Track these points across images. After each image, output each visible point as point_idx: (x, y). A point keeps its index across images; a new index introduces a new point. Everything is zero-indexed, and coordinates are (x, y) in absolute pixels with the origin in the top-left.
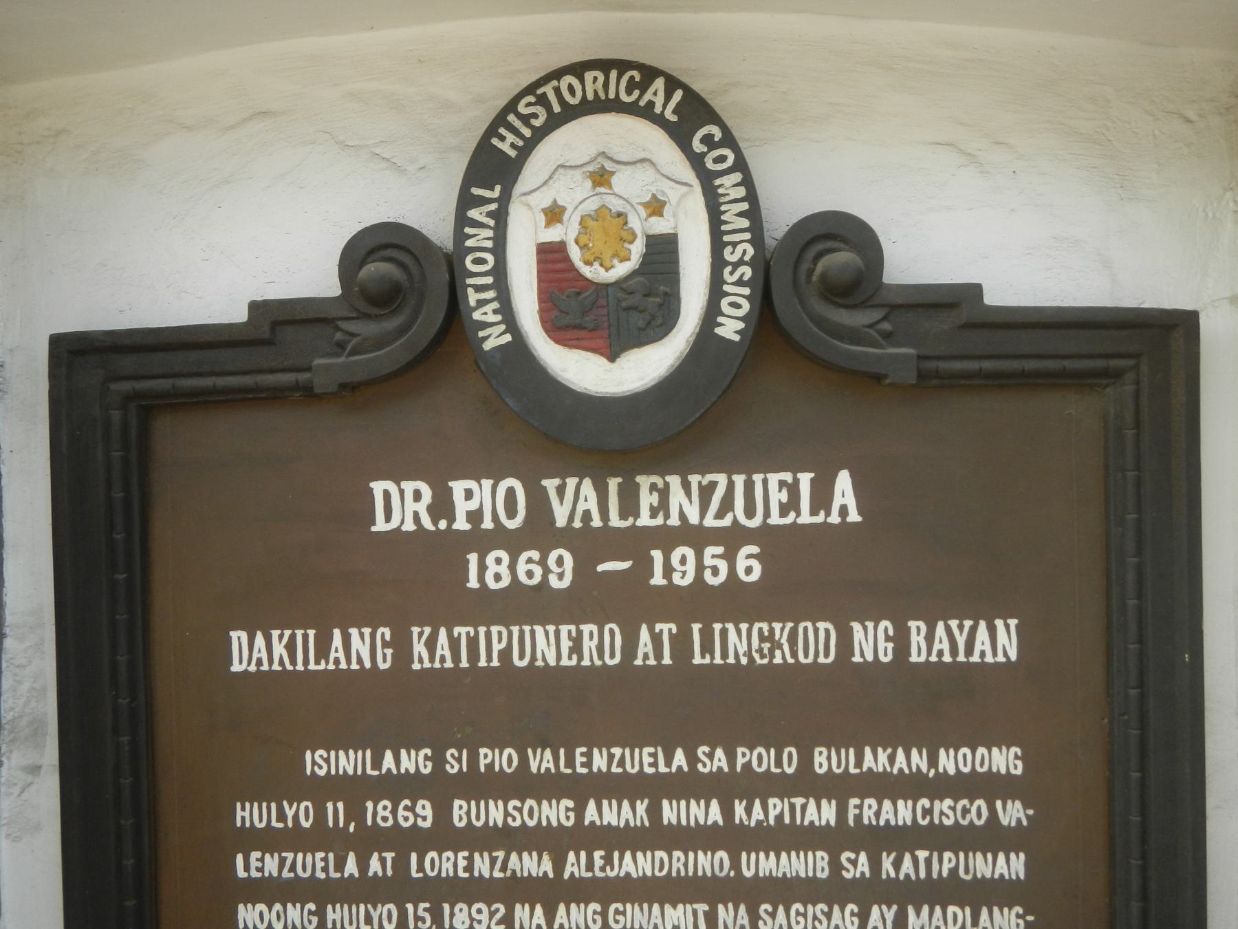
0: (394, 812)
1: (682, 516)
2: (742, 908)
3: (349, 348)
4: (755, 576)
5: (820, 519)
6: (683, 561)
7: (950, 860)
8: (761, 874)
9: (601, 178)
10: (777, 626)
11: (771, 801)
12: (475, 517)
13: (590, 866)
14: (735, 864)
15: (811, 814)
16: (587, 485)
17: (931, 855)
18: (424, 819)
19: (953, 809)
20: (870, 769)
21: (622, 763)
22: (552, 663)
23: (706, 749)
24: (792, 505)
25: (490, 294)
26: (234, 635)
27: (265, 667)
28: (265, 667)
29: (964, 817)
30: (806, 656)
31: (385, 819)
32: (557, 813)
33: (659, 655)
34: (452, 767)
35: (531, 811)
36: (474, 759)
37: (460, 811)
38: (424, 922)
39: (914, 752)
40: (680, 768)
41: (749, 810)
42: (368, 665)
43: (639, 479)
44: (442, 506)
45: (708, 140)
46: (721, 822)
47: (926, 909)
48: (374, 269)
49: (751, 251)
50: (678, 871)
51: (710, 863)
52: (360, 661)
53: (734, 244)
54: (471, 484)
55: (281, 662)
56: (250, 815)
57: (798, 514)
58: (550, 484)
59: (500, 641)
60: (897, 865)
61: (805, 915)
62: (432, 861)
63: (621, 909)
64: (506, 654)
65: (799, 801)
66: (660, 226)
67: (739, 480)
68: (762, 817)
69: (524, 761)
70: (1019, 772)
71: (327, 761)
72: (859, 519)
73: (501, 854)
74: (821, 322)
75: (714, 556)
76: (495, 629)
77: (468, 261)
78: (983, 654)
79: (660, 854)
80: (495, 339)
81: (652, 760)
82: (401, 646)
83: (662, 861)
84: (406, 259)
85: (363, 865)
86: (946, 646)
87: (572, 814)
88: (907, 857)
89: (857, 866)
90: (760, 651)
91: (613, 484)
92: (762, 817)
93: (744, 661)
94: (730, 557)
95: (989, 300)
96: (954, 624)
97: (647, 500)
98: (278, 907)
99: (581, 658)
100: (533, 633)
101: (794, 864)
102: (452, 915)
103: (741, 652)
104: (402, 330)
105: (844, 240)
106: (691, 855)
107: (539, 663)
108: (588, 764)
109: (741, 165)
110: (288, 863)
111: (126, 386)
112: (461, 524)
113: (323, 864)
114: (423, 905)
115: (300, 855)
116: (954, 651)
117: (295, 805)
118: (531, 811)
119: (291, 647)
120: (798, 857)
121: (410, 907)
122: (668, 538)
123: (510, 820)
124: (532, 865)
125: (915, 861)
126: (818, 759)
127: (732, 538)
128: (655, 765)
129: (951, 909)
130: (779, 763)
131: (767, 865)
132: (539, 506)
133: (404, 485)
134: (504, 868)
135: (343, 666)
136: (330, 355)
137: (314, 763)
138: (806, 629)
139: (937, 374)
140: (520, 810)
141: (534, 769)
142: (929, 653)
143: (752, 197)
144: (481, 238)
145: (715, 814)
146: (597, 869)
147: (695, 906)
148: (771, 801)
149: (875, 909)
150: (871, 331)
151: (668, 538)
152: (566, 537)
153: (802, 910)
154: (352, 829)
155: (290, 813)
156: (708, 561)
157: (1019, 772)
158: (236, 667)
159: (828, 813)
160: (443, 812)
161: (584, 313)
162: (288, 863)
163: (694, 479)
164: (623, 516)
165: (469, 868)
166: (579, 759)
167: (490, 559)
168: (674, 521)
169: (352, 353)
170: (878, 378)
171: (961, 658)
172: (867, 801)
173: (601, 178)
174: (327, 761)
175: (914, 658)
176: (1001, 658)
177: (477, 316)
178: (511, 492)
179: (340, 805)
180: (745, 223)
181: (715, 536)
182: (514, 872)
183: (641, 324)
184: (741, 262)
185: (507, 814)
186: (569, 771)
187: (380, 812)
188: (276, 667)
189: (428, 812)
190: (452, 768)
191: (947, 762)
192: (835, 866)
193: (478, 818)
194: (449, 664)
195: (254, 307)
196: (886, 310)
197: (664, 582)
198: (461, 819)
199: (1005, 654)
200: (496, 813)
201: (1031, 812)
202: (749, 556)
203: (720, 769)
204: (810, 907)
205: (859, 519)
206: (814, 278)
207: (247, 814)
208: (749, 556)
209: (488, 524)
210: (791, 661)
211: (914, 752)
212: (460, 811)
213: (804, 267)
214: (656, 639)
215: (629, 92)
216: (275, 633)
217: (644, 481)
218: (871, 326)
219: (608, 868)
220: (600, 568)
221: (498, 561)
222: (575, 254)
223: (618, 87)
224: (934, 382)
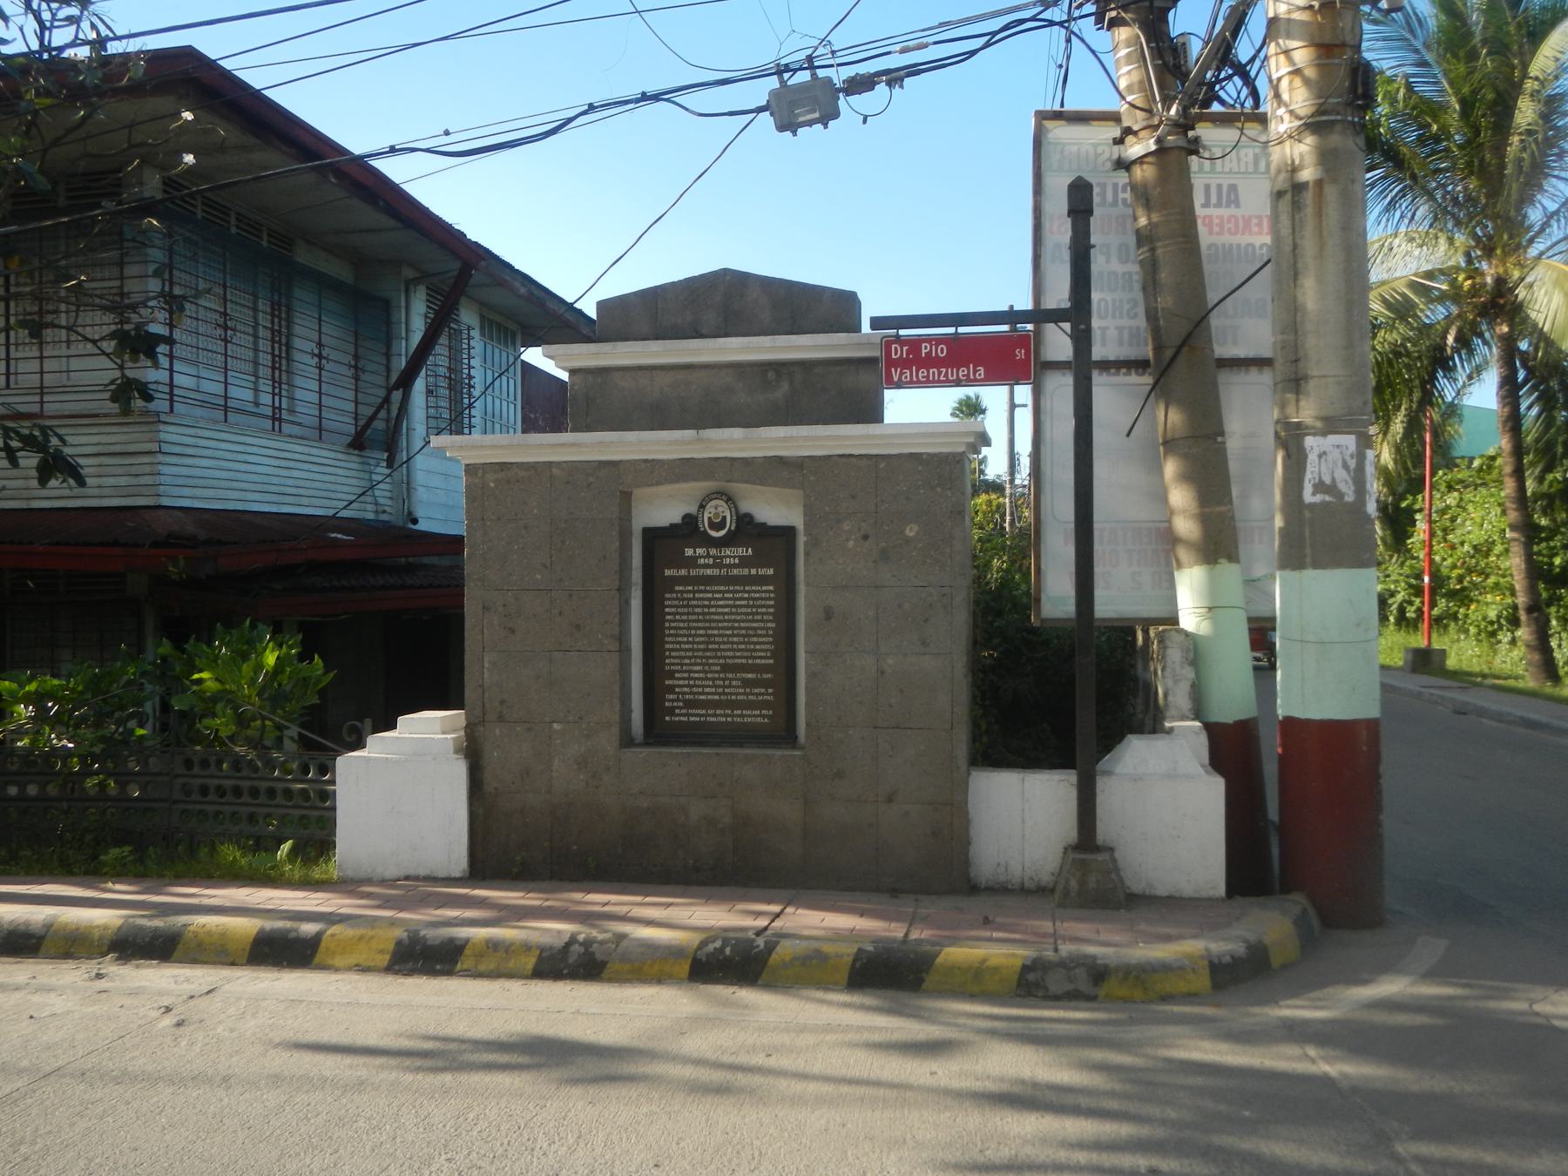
9: (716, 508)
32: (710, 595)
37: (697, 595)
51: (731, 602)
56: (667, 596)
82: (689, 572)
122: (726, 557)
124: (706, 603)
127: (734, 557)
131: (738, 603)
132: (708, 552)
151: (726, 557)
173: (716, 508)
187: (685, 595)
200: (701, 595)
223: (719, 496)
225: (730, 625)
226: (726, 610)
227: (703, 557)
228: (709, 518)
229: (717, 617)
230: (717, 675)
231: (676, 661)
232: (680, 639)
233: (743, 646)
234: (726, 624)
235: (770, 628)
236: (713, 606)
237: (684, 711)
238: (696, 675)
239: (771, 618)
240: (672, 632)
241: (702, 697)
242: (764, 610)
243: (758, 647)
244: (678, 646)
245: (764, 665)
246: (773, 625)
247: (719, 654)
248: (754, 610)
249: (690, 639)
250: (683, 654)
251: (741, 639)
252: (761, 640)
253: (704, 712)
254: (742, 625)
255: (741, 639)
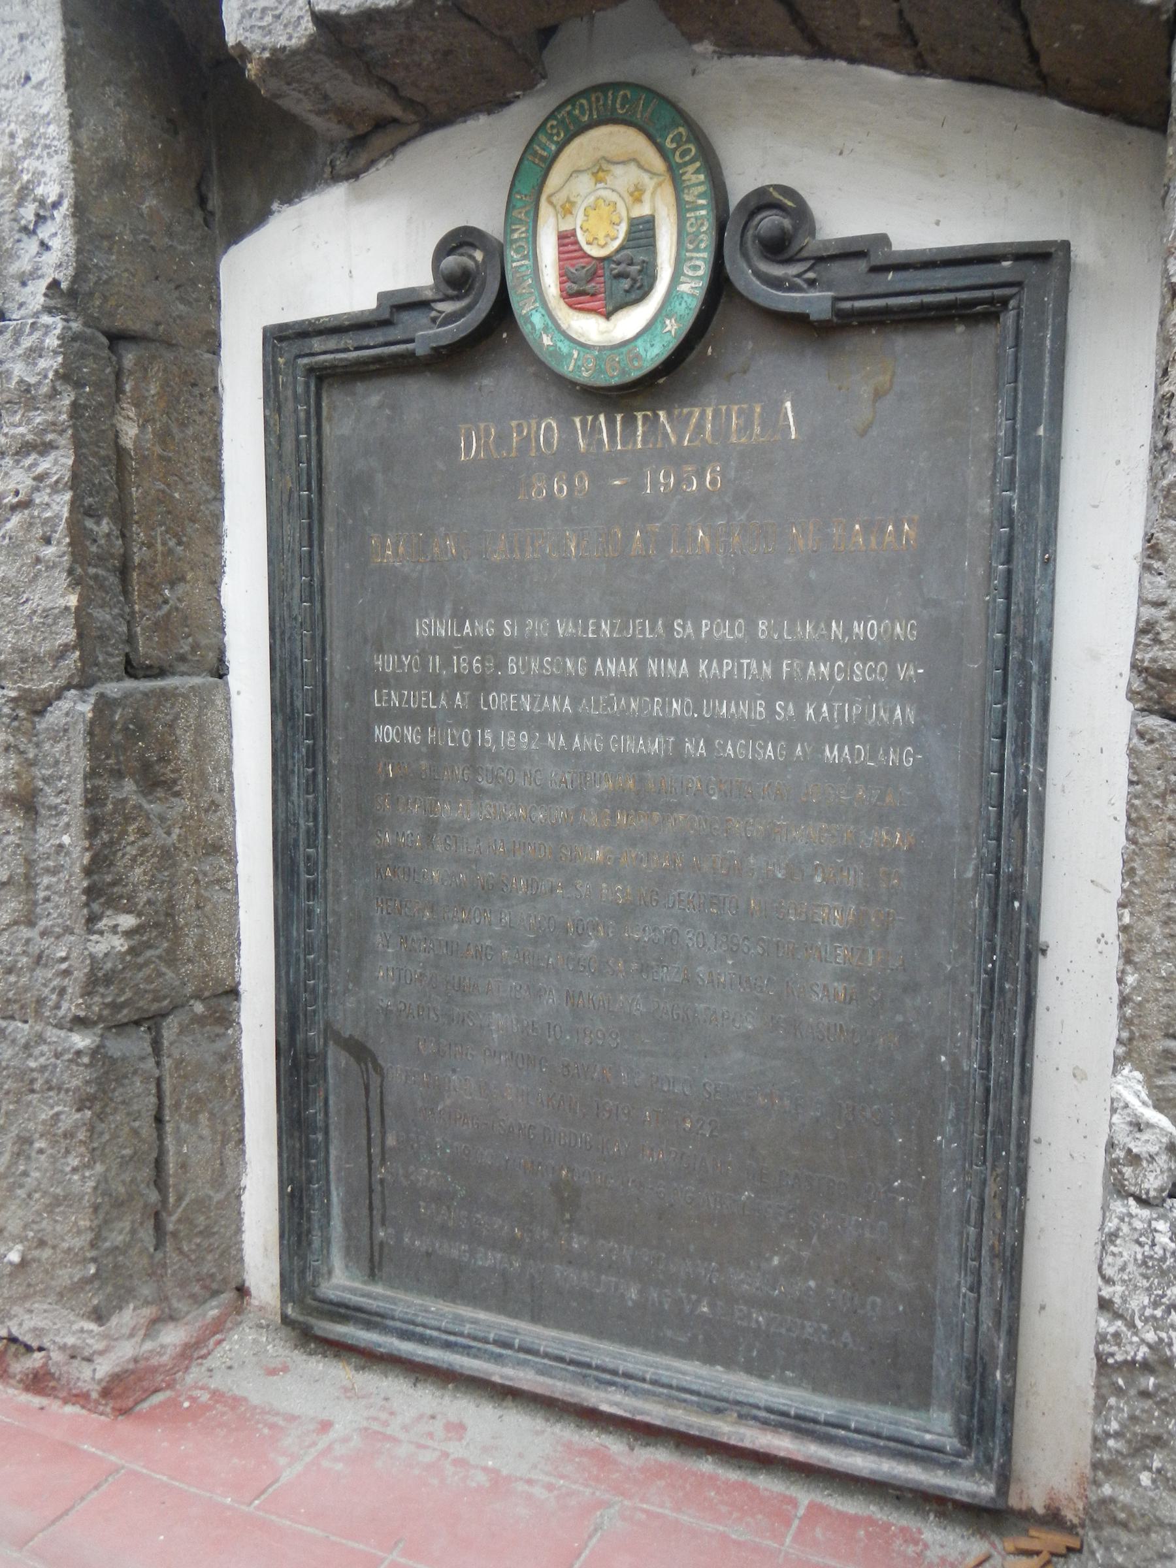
45: (677, 139)
48: (450, 262)
66: (644, 210)
95: (896, 247)
104: (469, 308)
111: (306, 361)
150: (798, 281)
183: (627, 287)
196: (812, 262)
203: (689, 635)
212: (513, 665)
215: (623, 107)
218: (799, 276)
222: (581, 238)
228: (566, 240)
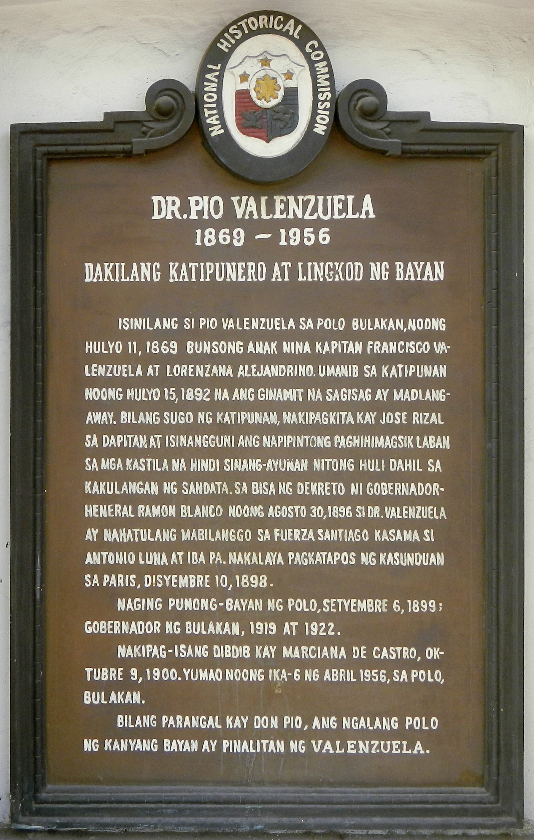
0: (160, 347)
1: (295, 214)
2: (319, 390)
3: (149, 134)
4: (327, 242)
5: (357, 216)
6: (295, 234)
7: (413, 369)
8: (328, 375)
10: (337, 264)
11: (333, 343)
12: (200, 213)
13: (250, 372)
14: (316, 371)
15: (351, 348)
16: (252, 199)
17: (404, 366)
18: (174, 350)
19: (415, 346)
20: (377, 328)
21: (265, 325)
22: (234, 279)
23: (304, 319)
24: (344, 210)
25: (215, 112)
26: (87, 265)
27: (101, 280)
28: (101, 280)
29: (419, 350)
30: (350, 277)
31: (155, 350)
33: (283, 277)
34: (187, 326)
35: (223, 346)
36: (197, 323)
38: (173, 397)
39: (397, 320)
40: (291, 327)
41: (323, 347)
42: (149, 279)
43: (275, 197)
44: (185, 208)
46: (310, 352)
47: (402, 391)
48: (164, 100)
49: (330, 96)
50: (290, 373)
51: (305, 370)
52: (145, 278)
53: (323, 93)
54: (199, 198)
55: (109, 278)
56: (92, 347)
57: (347, 214)
58: (235, 199)
59: (210, 269)
60: (389, 371)
61: (347, 394)
62: (177, 369)
63: (264, 391)
64: (213, 275)
65: (345, 343)
67: (321, 198)
68: (328, 350)
69: (220, 324)
70: (444, 329)
71: (129, 323)
72: (374, 216)
73: (209, 366)
74: (359, 127)
75: (308, 232)
76: (208, 264)
77: (205, 97)
78: (428, 277)
79: (281, 366)
80: (216, 131)
81: (279, 324)
82: (165, 272)
83: (282, 369)
84: (176, 95)
85: (145, 371)
86: (412, 273)
87: (242, 348)
88: (394, 367)
89: (371, 371)
90: (329, 275)
91: (264, 199)
92: (328, 350)
93: (321, 279)
94: (316, 233)
96: (416, 263)
97: (279, 207)
98: (104, 390)
99: (247, 278)
100: (225, 266)
101: (342, 371)
102: (186, 393)
103: (320, 276)
105: (370, 92)
106: (296, 367)
107: (228, 280)
108: (250, 326)
109: (326, 58)
110: (110, 370)
112: (194, 216)
113: (126, 370)
114: (172, 389)
115: (115, 366)
116: (416, 276)
117: (114, 343)
118: (223, 346)
119: (113, 271)
120: (345, 367)
121: (166, 390)
122: (288, 224)
123: (213, 350)
124: (223, 371)
125: (397, 369)
126: (354, 324)
127: (317, 225)
128: (280, 326)
129: (413, 391)
130: (336, 326)
131: (331, 371)
132: (229, 208)
133: (167, 198)
134: (210, 373)
135: (137, 280)
136: (139, 137)
137: (123, 324)
138: (349, 266)
139: (410, 152)
140: (218, 346)
141: (225, 328)
142: (405, 277)
143: (331, 72)
144: (211, 87)
145: (307, 348)
146: (253, 373)
147: (297, 390)
148: (333, 343)
149: (379, 390)
151: (288, 224)
152: (241, 223)
153: (346, 391)
154: (140, 354)
155: (111, 347)
156: (306, 235)
157: (444, 329)
158: (87, 280)
159: (359, 348)
160: (182, 347)
161: (257, 120)
162: (110, 370)
163: (300, 198)
164: (268, 214)
165: (194, 372)
166: (246, 323)
167: (207, 232)
168: (291, 216)
169: (151, 136)
170: (383, 153)
171: (419, 279)
172: (376, 343)
174: (129, 323)
175: (398, 279)
176: (436, 279)
177: (208, 121)
178: (217, 202)
179: (135, 343)
180: (328, 83)
181: (309, 224)
182: (215, 374)
184: (326, 100)
185: (212, 348)
186: (241, 329)
187: (153, 347)
188: (106, 280)
189: (176, 347)
190: (187, 327)
191: (412, 325)
192: (361, 371)
193: (198, 350)
194: (186, 280)
195: (106, 114)
197: (286, 244)
198: (190, 350)
199: (438, 277)
201: (449, 347)
202: (324, 233)
203: (310, 328)
204: (349, 390)
205: (374, 216)
206: (357, 108)
207: (91, 347)
208: (324, 233)
209: (206, 216)
210: (342, 279)
211: (397, 320)
213: (353, 103)
214: (282, 269)
216: (106, 265)
217: (277, 198)
219: (258, 373)
220: (257, 237)
221: (210, 233)
224: (409, 155)
225: (300, 441)
226: (289, 394)
227: (212, 223)
229: (258, 418)
230: (257, 605)
231: (120, 558)
232: (133, 488)
233: (346, 511)
234: (288, 440)
235: (436, 453)
236: (245, 383)
237: (149, 721)
238: (188, 604)
239: (435, 419)
240: (107, 464)
241: (203, 675)
242: (414, 395)
243: (392, 513)
244: (127, 512)
245: (410, 569)
246: (445, 443)
247: (264, 535)
248: (381, 395)
249: (169, 488)
250: (145, 535)
251: (339, 488)
252: (402, 489)
253: (212, 722)
254: (342, 441)
255: (339, 488)
